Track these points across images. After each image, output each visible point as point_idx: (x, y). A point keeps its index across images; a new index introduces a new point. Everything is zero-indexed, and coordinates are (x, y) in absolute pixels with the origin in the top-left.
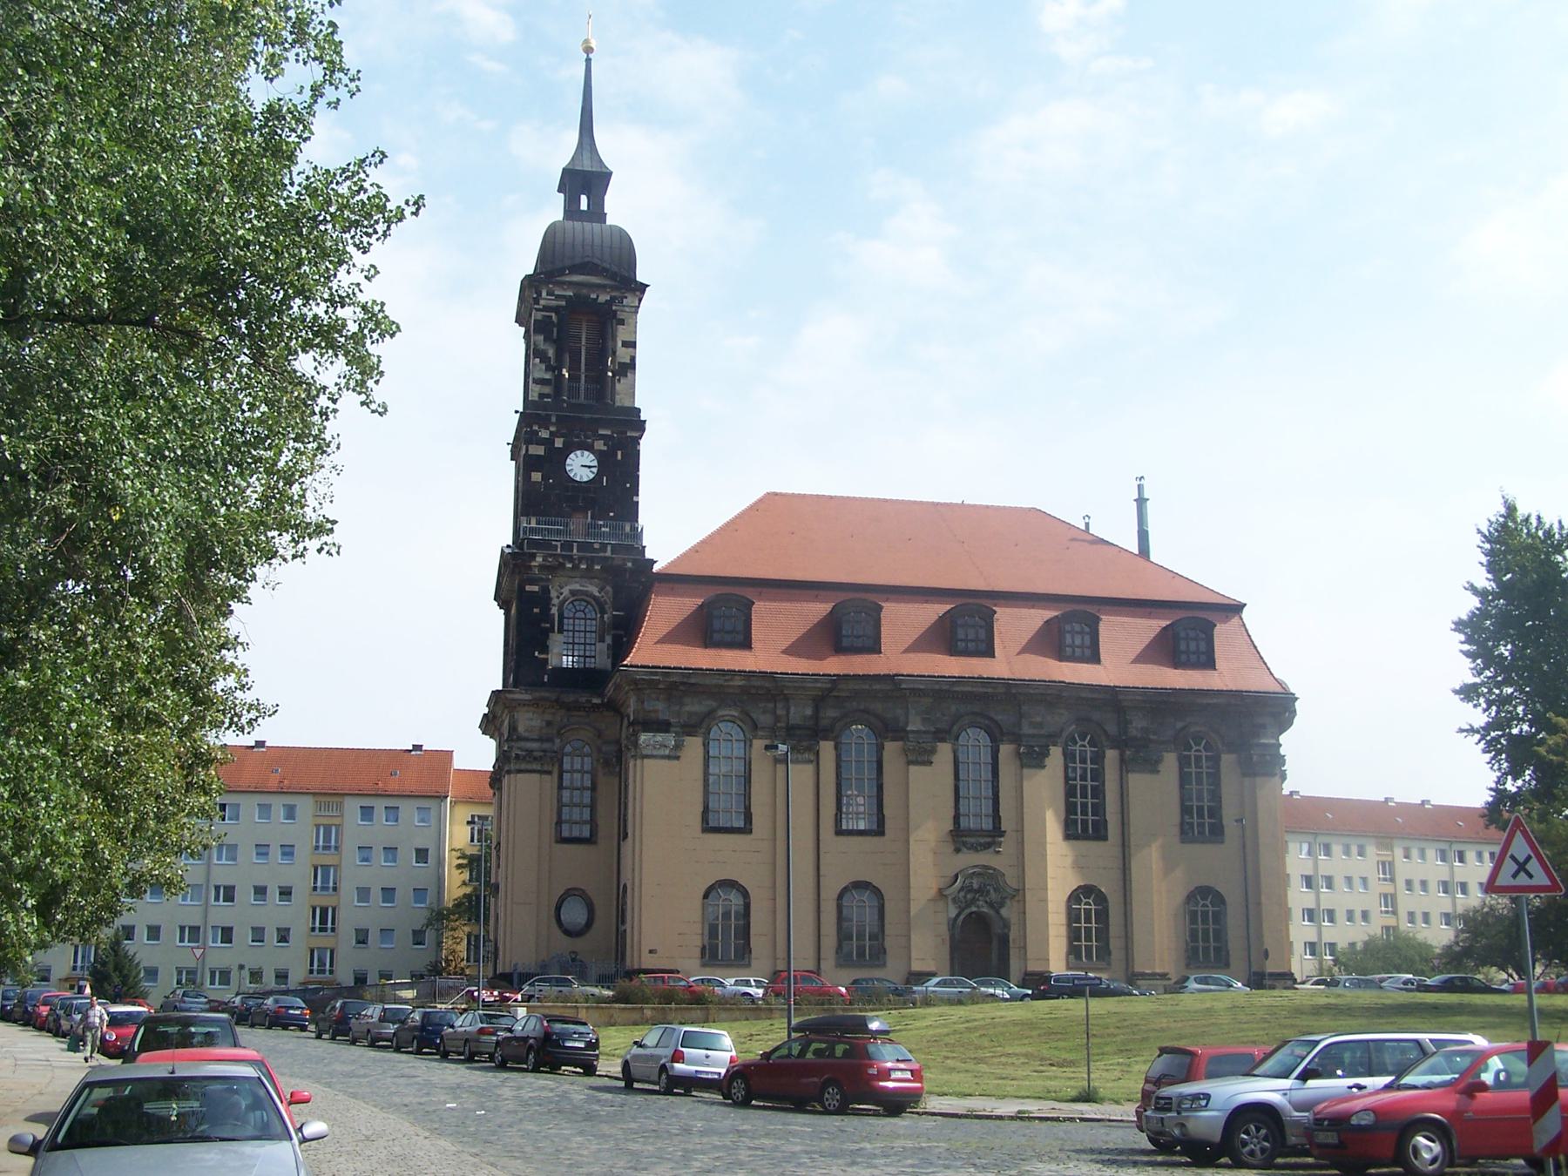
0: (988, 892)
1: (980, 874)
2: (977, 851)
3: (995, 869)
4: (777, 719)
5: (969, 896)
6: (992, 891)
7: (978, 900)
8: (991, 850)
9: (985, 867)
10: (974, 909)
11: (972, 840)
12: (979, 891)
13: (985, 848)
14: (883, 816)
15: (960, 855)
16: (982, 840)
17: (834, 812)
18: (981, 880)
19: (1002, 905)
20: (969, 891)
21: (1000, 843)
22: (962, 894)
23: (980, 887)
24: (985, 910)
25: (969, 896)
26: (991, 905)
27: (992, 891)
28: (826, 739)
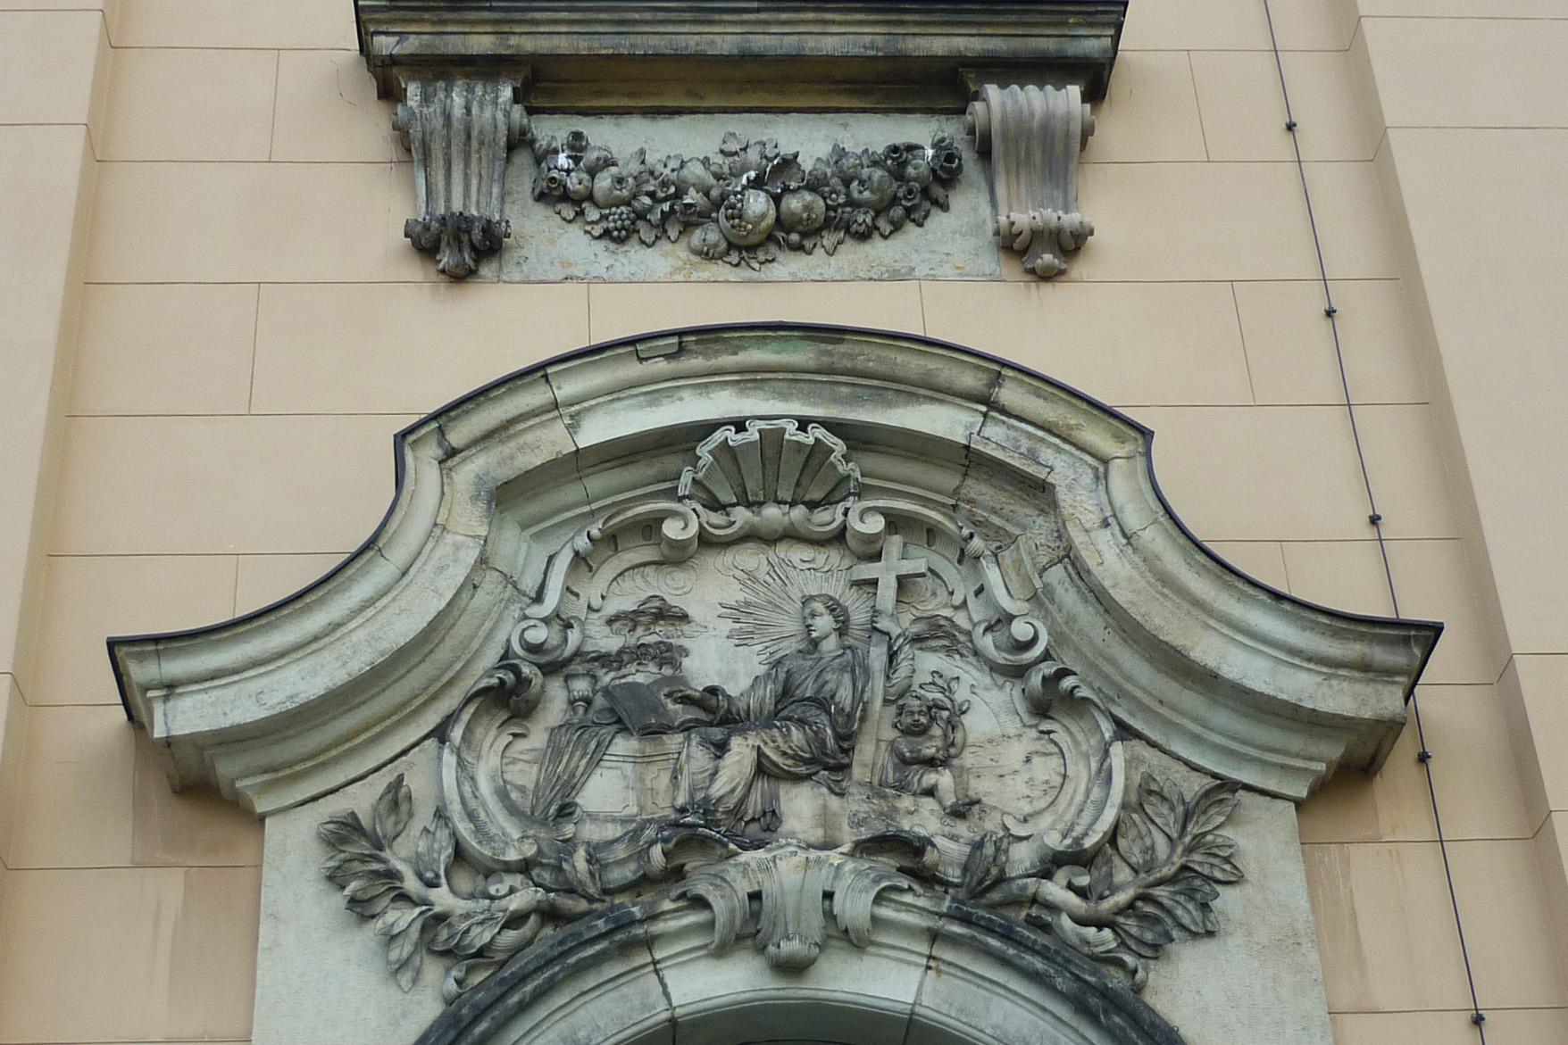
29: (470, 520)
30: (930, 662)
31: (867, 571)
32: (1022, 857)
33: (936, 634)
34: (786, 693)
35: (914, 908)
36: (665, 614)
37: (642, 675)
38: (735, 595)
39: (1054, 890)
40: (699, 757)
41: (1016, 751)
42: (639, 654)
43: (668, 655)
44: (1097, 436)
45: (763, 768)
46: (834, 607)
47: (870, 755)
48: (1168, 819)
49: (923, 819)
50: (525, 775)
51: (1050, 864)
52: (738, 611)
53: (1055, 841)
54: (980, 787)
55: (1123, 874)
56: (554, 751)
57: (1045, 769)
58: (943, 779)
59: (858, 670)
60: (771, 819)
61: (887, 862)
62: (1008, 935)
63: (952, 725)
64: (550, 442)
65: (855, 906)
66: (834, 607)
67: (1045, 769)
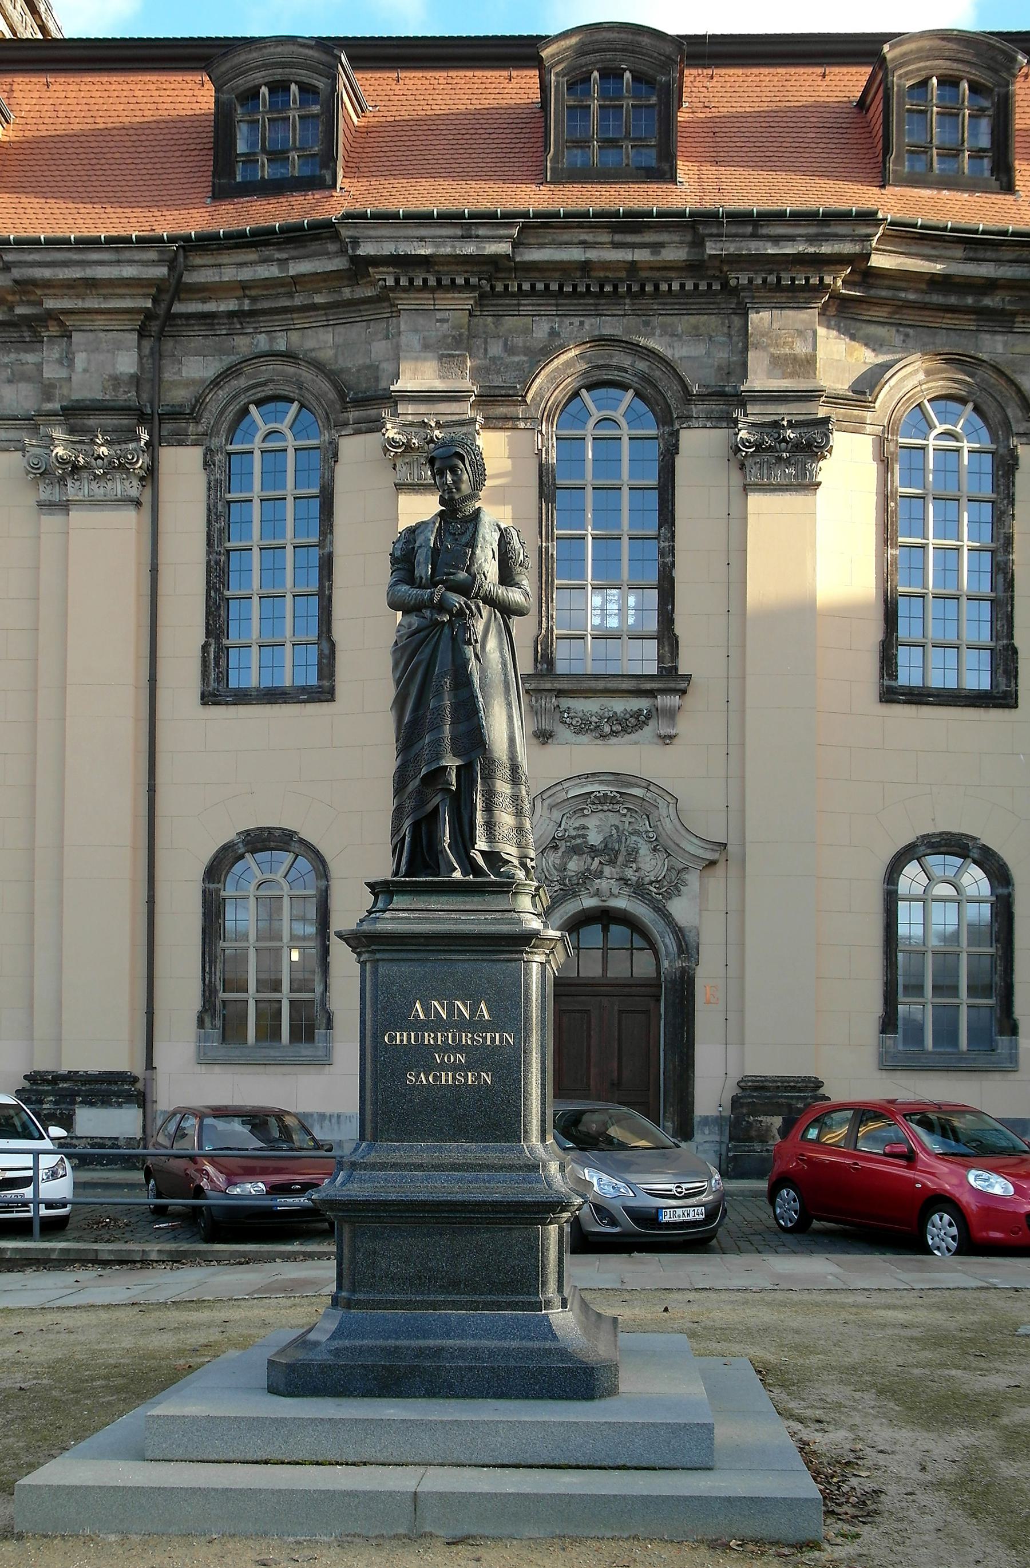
0: (632, 855)
1: (604, 799)
2: (603, 736)
3: (648, 785)
4: (47, 391)
5: (574, 865)
6: (644, 849)
7: (599, 875)
8: (648, 731)
9: (617, 777)
10: (589, 902)
11: (590, 706)
12: (608, 852)
13: (626, 729)
14: (333, 645)
15: (552, 750)
16: (620, 706)
17: (201, 639)
18: (614, 819)
19: (674, 889)
20: (576, 850)
21: (671, 714)
22: (554, 858)
23: (605, 842)
24: (621, 903)
25: (574, 865)
26: (639, 890)
27: (644, 849)
28: (179, 440)
29: (546, 812)
30: (634, 838)
31: (623, 819)
32: (647, 880)
33: (636, 833)
34: (606, 846)
35: (626, 890)
36: (584, 828)
37: (579, 841)
38: (598, 823)
39: (652, 888)
40: (589, 860)
41: (648, 859)
42: (579, 836)
43: (584, 836)
44: (668, 798)
45: (600, 863)
46: (617, 828)
47: (621, 859)
48: (675, 873)
49: (629, 873)
50: (558, 861)
51: (651, 883)
52: (597, 827)
53: (653, 879)
54: (641, 865)
55: (665, 883)
56: (563, 856)
57: (653, 862)
58: (634, 865)
59: (620, 842)
60: (602, 872)
61: (622, 882)
62: (642, 896)
63: (637, 852)
64: (563, 796)
65: (615, 891)
66: (617, 828)
67: (653, 862)
